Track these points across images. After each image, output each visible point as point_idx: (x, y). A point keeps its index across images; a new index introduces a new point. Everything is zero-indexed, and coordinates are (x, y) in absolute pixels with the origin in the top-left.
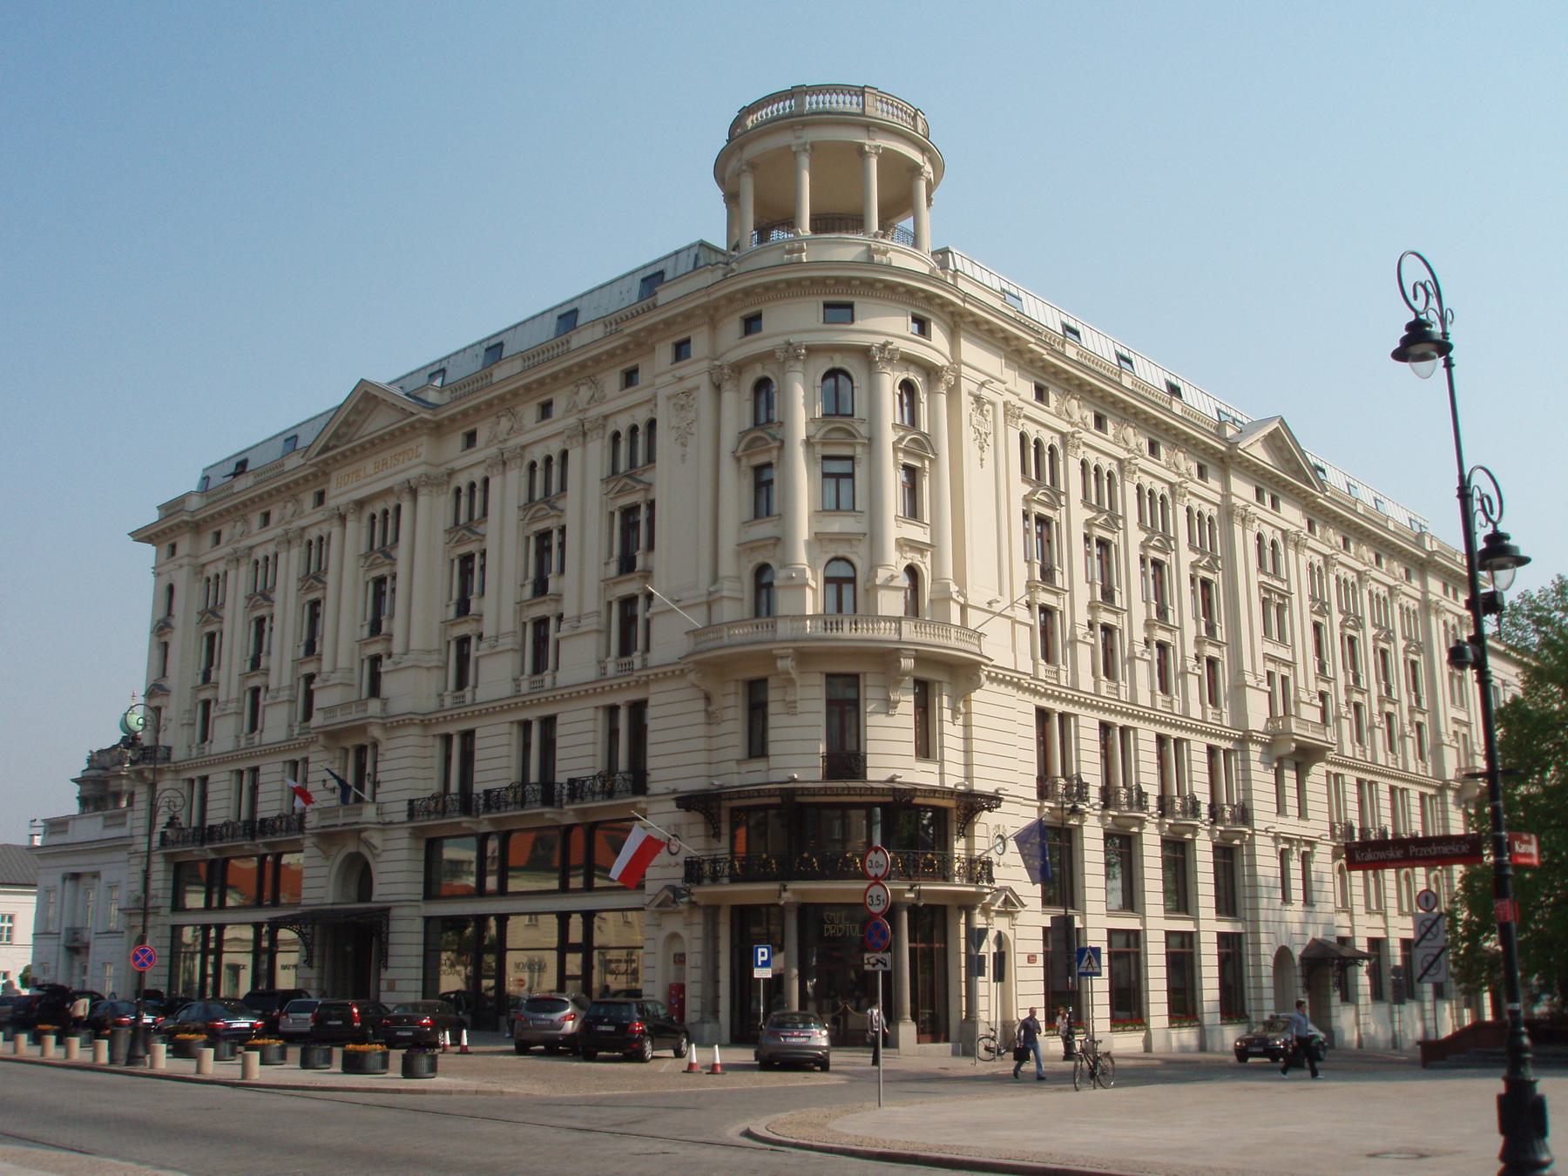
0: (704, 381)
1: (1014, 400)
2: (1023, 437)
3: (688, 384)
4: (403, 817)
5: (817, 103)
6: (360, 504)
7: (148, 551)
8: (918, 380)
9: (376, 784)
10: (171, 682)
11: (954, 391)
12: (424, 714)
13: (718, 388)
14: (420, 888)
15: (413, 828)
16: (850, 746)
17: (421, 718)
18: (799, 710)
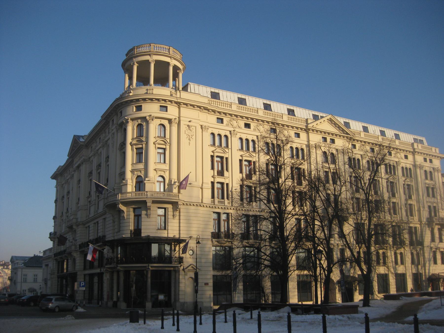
0: (115, 130)
1: (201, 124)
2: (213, 134)
3: (113, 132)
4: (78, 249)
5: (140, 50)
6: (78, 167)
7: (54, 182)
8: (166, 123)
9: (76, 240)
10: (57, 216)
11: (179, 124)
12: (83, 222)
13: (117, 131)
14: (83, 267)
15: (80, 251)
16: (139, 228)
17: (82, 223)
18: (151, 217)
